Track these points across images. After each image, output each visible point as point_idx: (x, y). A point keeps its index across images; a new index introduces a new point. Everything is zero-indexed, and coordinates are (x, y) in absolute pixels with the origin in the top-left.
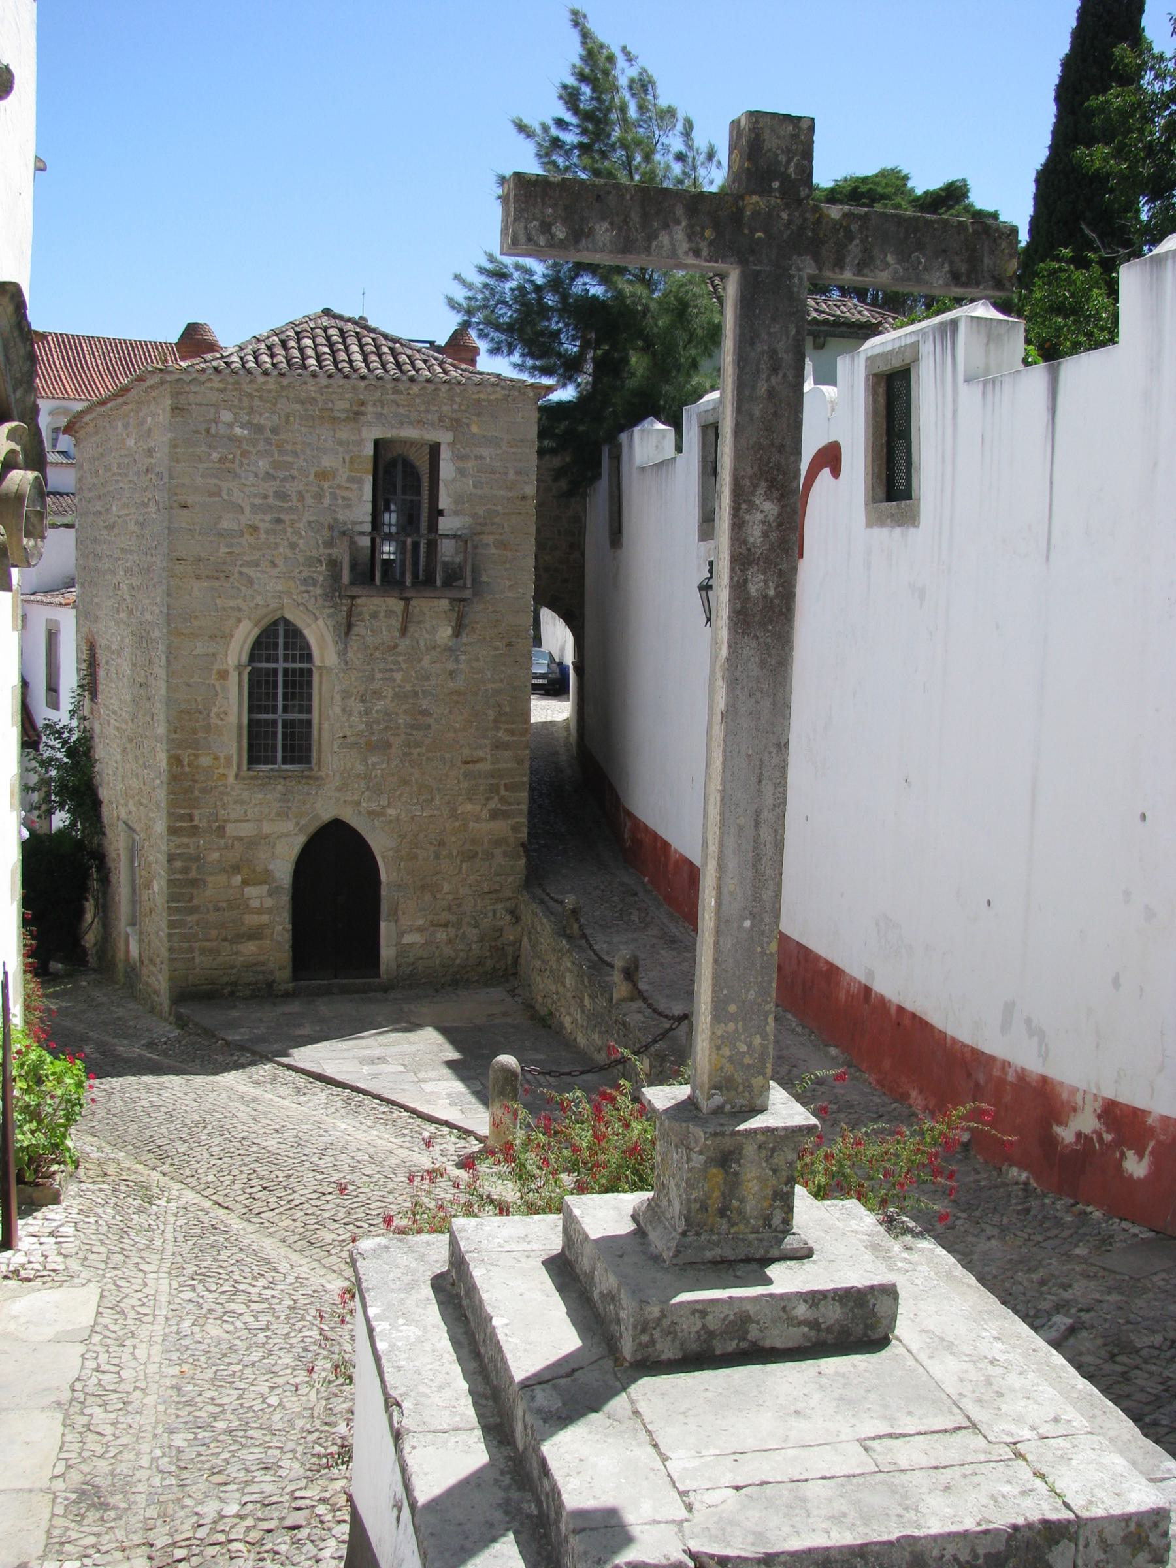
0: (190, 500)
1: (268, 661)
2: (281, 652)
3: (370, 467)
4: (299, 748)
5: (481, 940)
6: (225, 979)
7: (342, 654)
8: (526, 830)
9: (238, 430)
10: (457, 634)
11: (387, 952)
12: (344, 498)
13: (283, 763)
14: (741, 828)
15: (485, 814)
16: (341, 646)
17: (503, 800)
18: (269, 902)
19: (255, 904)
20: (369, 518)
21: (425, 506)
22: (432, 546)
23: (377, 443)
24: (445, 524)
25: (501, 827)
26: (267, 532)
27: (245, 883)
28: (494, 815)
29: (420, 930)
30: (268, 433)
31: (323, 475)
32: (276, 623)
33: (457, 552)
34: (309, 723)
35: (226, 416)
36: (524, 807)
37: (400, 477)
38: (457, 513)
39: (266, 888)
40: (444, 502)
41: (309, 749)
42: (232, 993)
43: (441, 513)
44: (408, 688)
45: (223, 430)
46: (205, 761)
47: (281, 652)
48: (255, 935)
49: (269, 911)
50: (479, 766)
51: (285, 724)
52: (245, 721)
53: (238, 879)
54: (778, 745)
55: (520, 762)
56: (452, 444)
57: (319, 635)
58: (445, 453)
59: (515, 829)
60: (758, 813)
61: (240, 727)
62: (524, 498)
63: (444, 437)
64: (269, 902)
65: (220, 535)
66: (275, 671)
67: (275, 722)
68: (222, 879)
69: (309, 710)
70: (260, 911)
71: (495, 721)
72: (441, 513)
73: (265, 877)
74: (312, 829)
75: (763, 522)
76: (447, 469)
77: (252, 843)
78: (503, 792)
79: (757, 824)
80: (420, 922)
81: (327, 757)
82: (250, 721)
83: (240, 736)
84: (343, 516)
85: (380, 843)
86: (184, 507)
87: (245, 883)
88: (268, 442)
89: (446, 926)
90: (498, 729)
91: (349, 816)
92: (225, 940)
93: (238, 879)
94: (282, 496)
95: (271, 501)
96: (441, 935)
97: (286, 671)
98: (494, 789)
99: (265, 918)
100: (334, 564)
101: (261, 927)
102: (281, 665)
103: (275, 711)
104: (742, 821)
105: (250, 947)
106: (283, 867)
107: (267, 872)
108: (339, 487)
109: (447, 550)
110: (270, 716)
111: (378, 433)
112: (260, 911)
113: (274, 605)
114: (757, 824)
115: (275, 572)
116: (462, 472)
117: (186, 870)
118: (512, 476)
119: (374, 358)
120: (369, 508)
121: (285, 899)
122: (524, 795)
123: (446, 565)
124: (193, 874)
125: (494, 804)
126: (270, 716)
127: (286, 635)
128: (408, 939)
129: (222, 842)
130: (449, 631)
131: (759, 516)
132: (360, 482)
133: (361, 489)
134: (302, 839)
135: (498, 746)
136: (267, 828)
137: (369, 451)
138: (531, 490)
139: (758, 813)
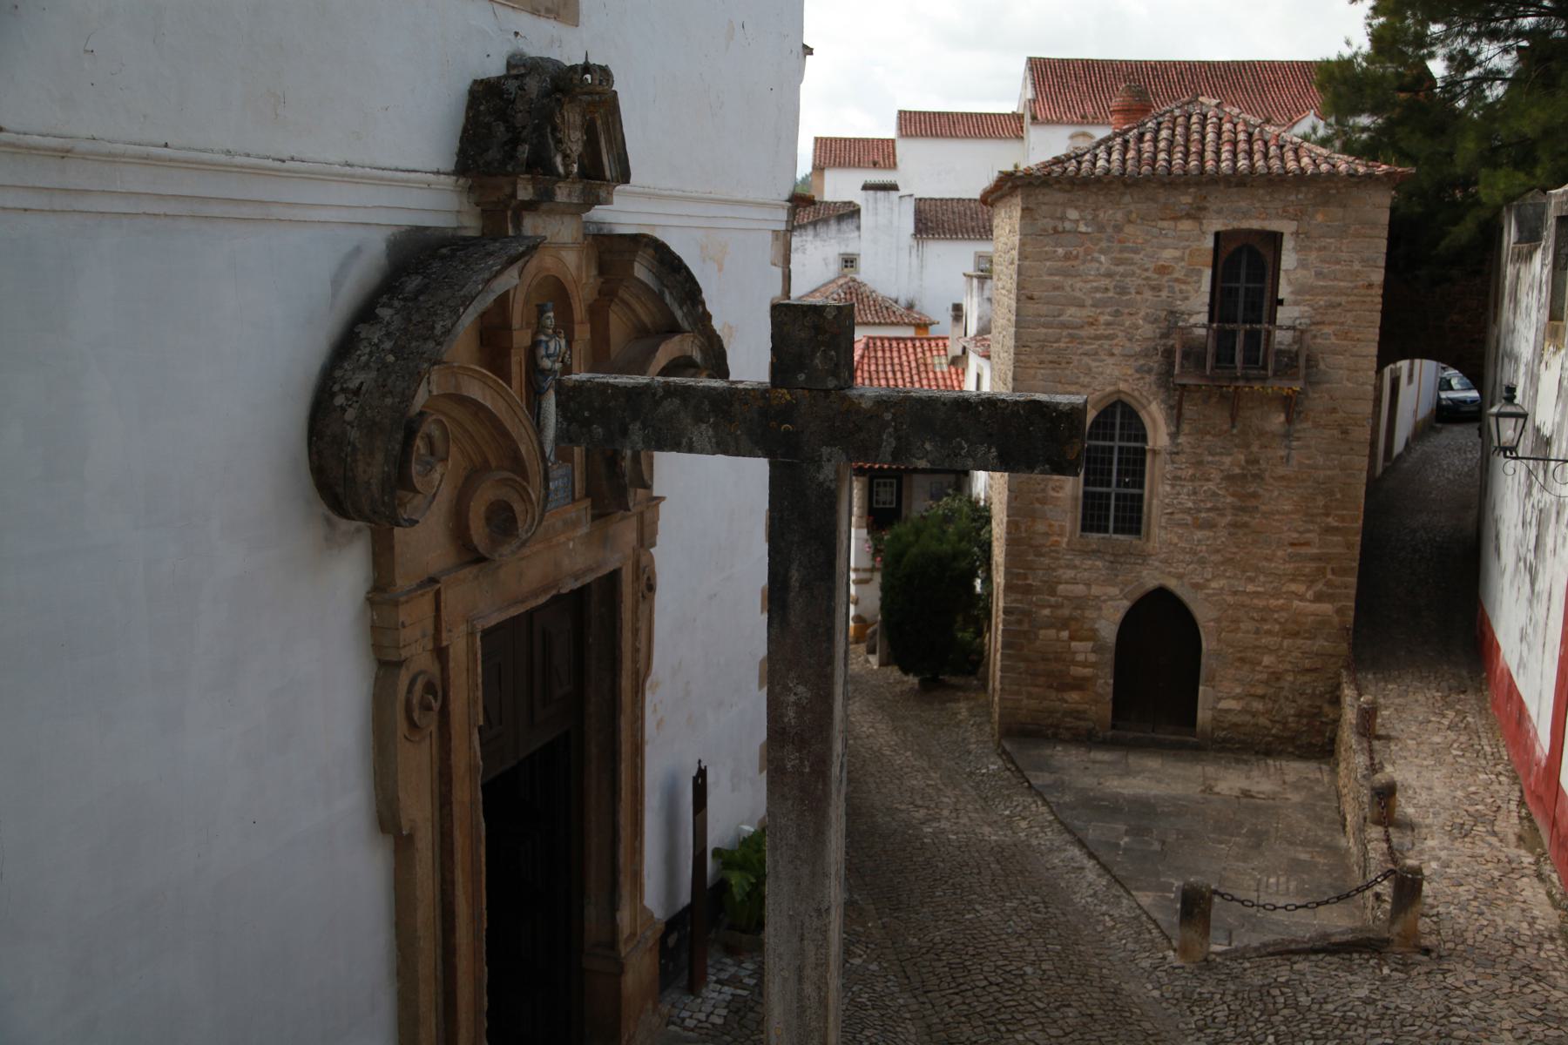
0: (1036, 294)
1: (1104, 439)
2: (1117, 432)
3: (1210, 259)
4: (1131, 518)
5: (1299, 715)
6: (1049, 721)
7: (1173, 436)
8: (1352, 613)
9: (1083, 228)
10: (1289, 420)
11: (1203, 715)
12: (1181, 291)
13: (1116, 531)
14: (785, 980)
15: (1309, 595)
16: (1173, 429)
17: (1328, 584)
18: (1092, 658)
19: (1081, 657)
20: (1206, 309)
21: (1268, 295)
22: (1269, 333)
23: (1217, 235)
24: (1284, 315)
25: (1326, 608)
26: (1108, 324)
27: (1072, 638)
28: (1319, 598)
29: (1237, 698)
30: (1110, 230)
31: (1163, 270)
32: (1113, 405)
33: (1295, 342)
34: (1141, 497)
35: (1073, 214)
36: (1353, 592)
37: (1244, 269)
38: (1296, 303)
39: (1090, 644)
40: (1284, 291)
41: (1139, 520)
42: (1055, 735)
43: (1281, 302)
44: (1237, 471)
45: (1068, 226)
46: (1040, 527)
47: (1117, 432)
48: (1080, 684)
49: (1093, 665)
50: (1303, 550)
51: (1118, 497)
52: (1081, 493)
53: (1065, 634)
54: (818, 911)
55: (1349, 546)
56: (1296, 234)
57: (1155, 417)
58: (1288, 244)
59: (1339, 611)
60: (800, 969)
61: (1076, 499)
62: (1370, 286)
63: (1286, 227)
64: (1092, 658)
65: (1064, 326)
66: (1111, 449)
67: (1108, 495)
68: (1052, 633)
69: (1141, 486)
70: (1085, 665)
71: (1325, 506)
72: (1281, 302)
73: (1093, 635)
74: (1137, 595)
75: (795, 703)
76: (1288, 260)
77: (1080, 603)
78: (1329, 576)
79: (800, 980)
80: (1238, 690)
81: (1155, 531)
82: (1085, 493)
83: (1076, 507)
84: (1181, 306)
85: (1204, 614)
86: (1031, 298)
87: (1072, 638)
88: (1110, 239)
89: (1262, 697)
90: (1327, 515)
91: (1172, 584)
92: (1050, 687)
93: (1065, 634)
94: (1123, 290)
95: (1111, 294)
96: (1258, 706)
97: (1121, 448)
98: (1321, 572)
99: (1087, 671)
100: (1169, 353)
101: (1085, 679)
102: (1117, 444)
103: (1109, 484)
104: (786, 973)
105: (1074, 696)
106: (1108, 629)
107: (1095, 631)
108: (1177, 280)
109: (1282, 338)
110: (1104, 489)
111: (1218, 225)
112: (1085, 665)
113: (1109, 389)
114: (800, 980)
115: (1110, 361)
116: (1303, 264)
117: (1020, 622)
118: (1357, 266)
119: (1226, 147)
120: (1207, 299)
121: (1110, 656)
122: (1353, 580)
123: (1279, 353)
124: (1026, 627)
125: (1319, 586)
126: (1104, 489)
127: (1122, 417)
128: (1223, 705)
129: (1053, 599)
130: (1282, 418)
131: (792, 698)
132: (1199, 273)
133: (1199, 281)
134: (1127, 604)
135: (1328, 530)
136: (1095, 590)
137: (1209, 243)
138: (1378, 277)
139: (800, 969)
